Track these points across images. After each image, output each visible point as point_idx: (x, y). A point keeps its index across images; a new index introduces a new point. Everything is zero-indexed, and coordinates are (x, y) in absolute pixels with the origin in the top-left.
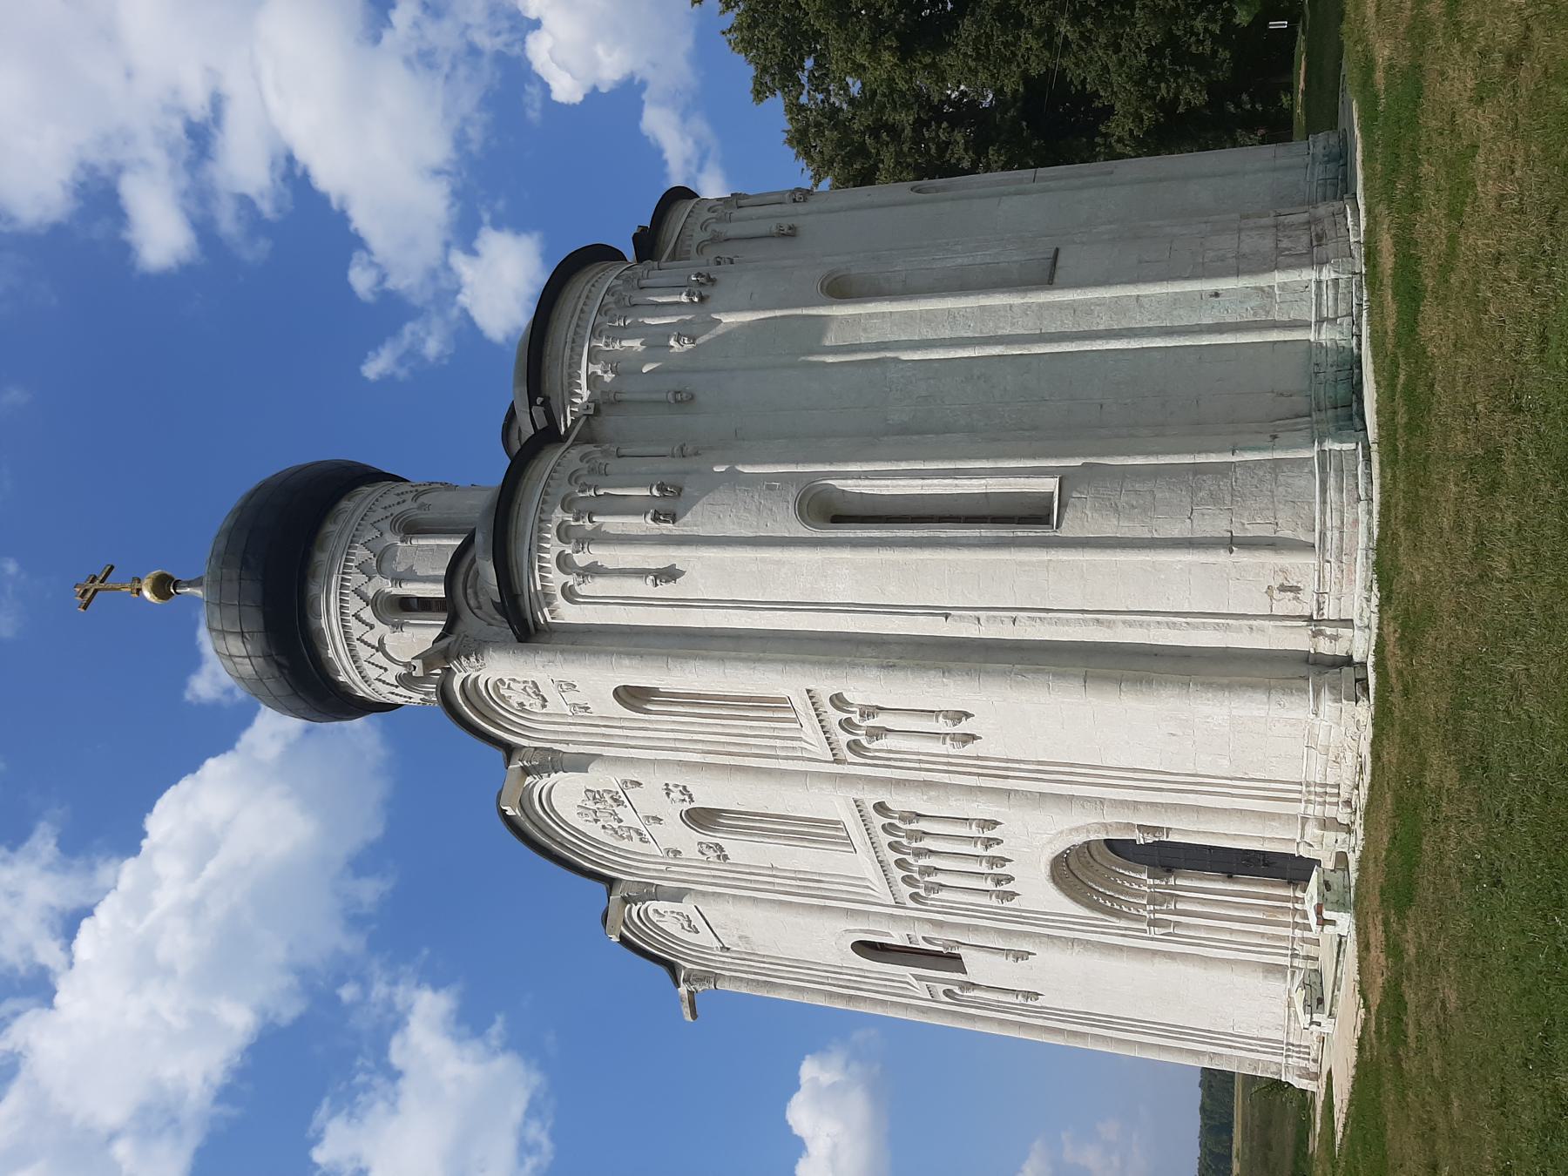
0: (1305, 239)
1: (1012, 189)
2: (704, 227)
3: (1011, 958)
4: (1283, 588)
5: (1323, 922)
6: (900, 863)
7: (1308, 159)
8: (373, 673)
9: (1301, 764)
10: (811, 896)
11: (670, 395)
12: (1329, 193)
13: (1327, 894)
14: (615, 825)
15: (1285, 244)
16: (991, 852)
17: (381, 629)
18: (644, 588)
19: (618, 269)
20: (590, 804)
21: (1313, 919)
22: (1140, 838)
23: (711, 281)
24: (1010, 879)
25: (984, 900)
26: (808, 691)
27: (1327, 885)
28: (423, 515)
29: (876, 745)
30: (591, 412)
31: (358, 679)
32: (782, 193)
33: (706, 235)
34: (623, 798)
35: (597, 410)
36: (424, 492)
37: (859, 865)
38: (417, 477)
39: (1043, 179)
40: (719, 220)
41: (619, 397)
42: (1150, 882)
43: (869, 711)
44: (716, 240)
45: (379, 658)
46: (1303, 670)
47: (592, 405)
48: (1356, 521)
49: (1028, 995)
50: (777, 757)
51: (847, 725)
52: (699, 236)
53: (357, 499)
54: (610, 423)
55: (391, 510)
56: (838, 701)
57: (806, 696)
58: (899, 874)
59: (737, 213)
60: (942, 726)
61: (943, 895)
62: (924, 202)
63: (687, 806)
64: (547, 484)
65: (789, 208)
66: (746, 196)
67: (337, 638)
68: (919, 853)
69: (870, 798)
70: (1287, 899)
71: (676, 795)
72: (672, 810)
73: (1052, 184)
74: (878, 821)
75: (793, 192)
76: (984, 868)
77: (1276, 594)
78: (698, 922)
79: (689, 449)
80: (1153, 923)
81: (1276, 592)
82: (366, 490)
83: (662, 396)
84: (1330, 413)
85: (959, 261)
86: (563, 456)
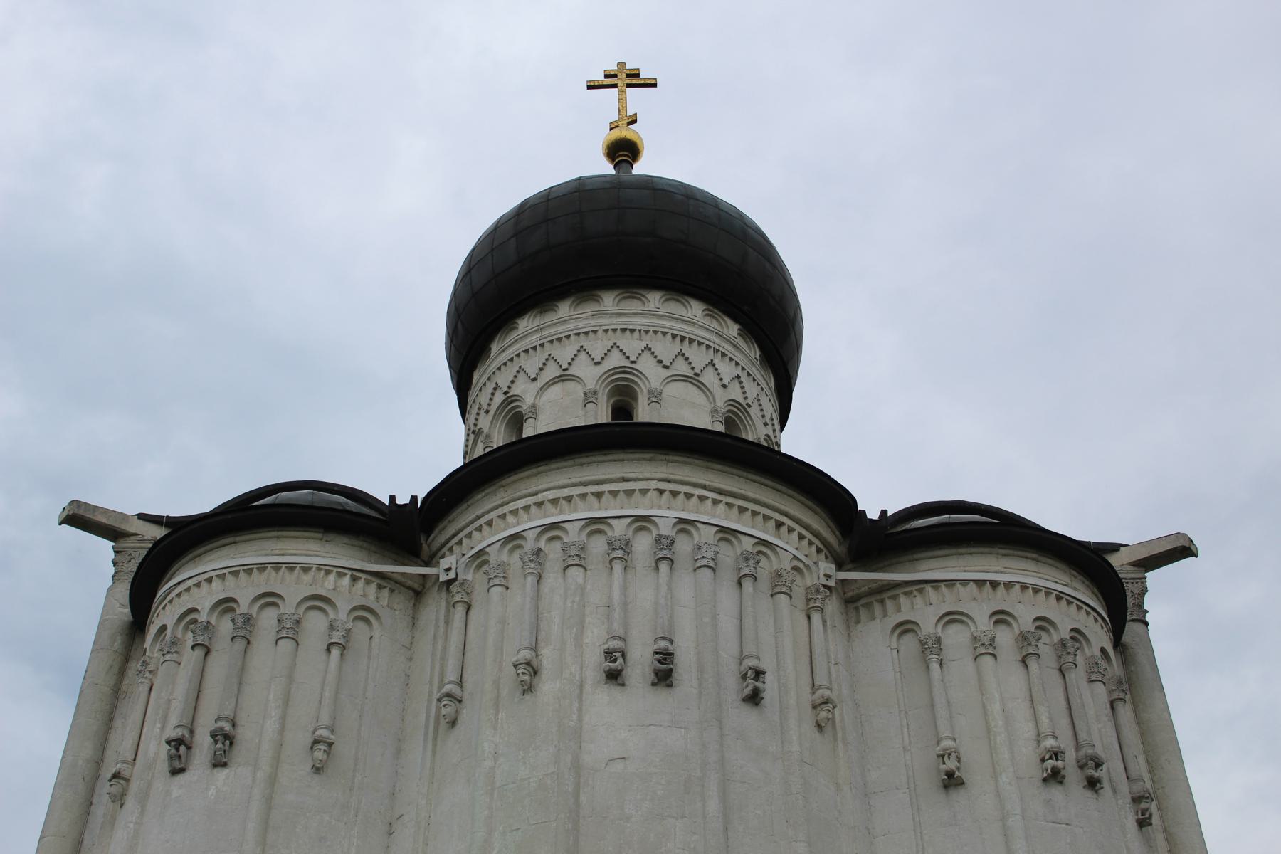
23: (664, 677)
45: (472, 436)
47: (452, 575)
64: (262, 567)
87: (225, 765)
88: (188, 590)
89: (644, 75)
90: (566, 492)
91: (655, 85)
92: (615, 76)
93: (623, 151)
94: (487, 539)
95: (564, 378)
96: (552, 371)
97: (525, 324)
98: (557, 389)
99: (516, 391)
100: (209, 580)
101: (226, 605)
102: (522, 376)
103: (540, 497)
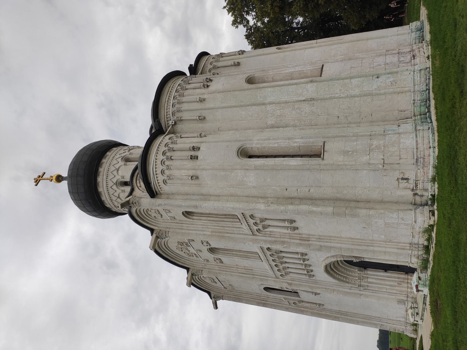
0: (409, 57)
1: (309, 46)
2: (211, 64)
3: (314, 295)
4: (403, 179)
5: (418, 291)
6: (276, 265)
7: (410, 31)
11: (198, 118)
12: (417, 41)
13: (420, 281)
14: (188, 252)
15: (402, 59)
17: (119, 191)
19: (183, 78)
20: (180, 246)
21: (415, 290)
22: (355, 261)
23: (211, 80)
24: (312, 271)
25: (304, 277)
26: (242, 213)
27: (420, 278)
28: (130, 156)
29: (266, 230)
30: (173, 124)
31: (113, 206)
32: (236, 52)
33: (211, 67)
35: (175, 123)
36: (132, 149)
37: (263, 266)
38: (131, 144)
39: (319, 43)
40: (216, 61)
41: (182, 118)
43: (262, 220)
44: (215, 67)
46: (411, 207)
47: (174, 122)
48: (429, 155)
49: (320, 305)
50: (234, 234)
51: (256, 224)
52: (210, 67)
53: (112, 152)
54: (179, 127)
55: (121, 155)
57: (242, 215)
58: (276, 269)
59: (221, 59)
60: (286, 224)
61: (291, 275)
62: (280, 52)
63: (209, 247)
64: (158, 147)
65: (238, 56)
66: (224, 54)
67: (106, 194)
68: (282, 263)
69: (265, 246)
70: (405, 279)
71: (205, 244)
72: (205, 248)
73: (322, 44)
74: (268, 253)
75: (239, 51)
77: (400, 181)
78: (216, 280)
79: (203, 135)
80: (360, 286)
81: (400, 180)
82: (115, 149)
83: (195, 118)
84: (419, 117)
85: (290, 71)
86: (164, 138)
87: (200, 148)
88: (156, 165)
89: (41, 175)
90: (168, 96)
91: (45, 173)
92: (37, 180)
93: (59, 179)
94: (171, 110)
95: (118, 170)
96: (115, 173)
97: (99, 179)
98: (119, 172)
99: (115, 180)
100: (156, 159)
101: (164, 153)
102: (112, 180)
103: (166, 101)
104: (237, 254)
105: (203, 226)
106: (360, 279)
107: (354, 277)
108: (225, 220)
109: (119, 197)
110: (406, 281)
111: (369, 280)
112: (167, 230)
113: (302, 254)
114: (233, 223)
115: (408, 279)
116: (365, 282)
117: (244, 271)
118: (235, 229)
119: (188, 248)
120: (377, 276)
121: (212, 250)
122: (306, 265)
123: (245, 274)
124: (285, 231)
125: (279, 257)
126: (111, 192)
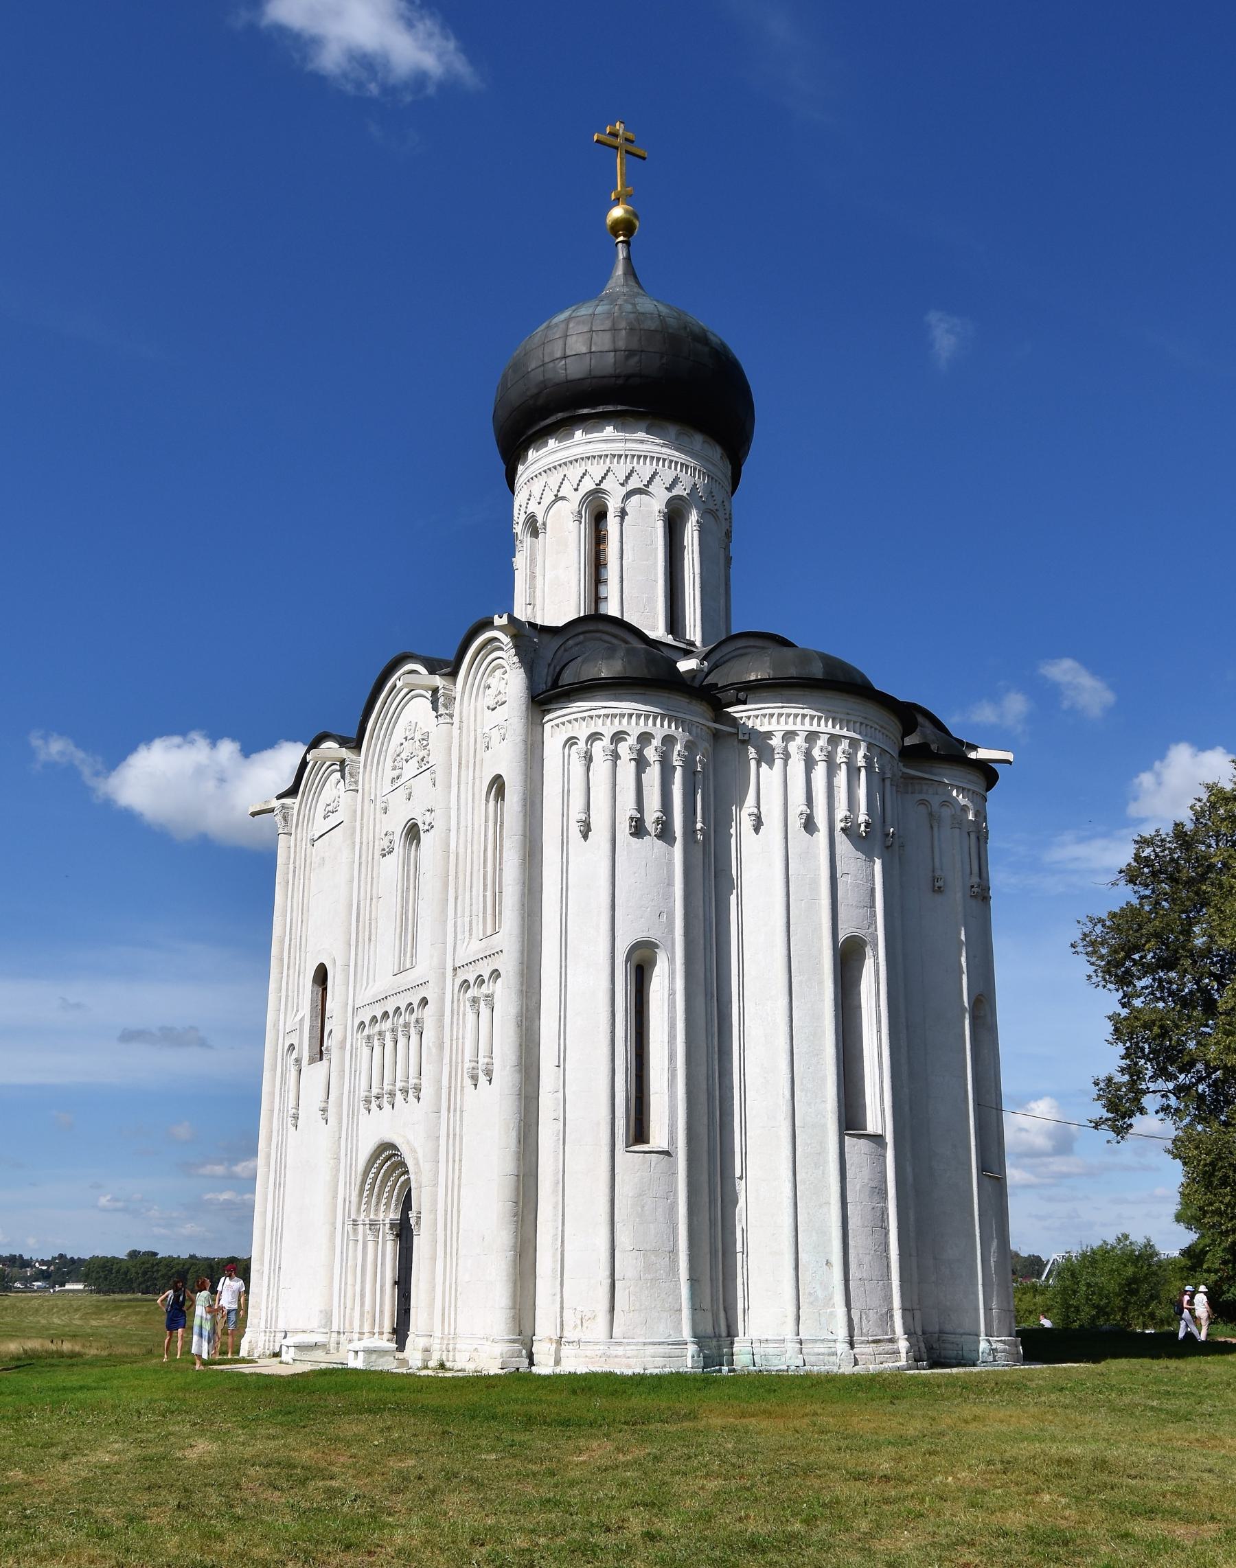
3: (323, 1105)
6: (386, 1014)
8: (536, 487)
9: (464, 1333)
10: (359, 932)
14: (403, 756)
16: (398, 1093)
18: (576, 813)
20: (418, 736)
34: (424, 768)
42: (387, 1221)
43: (489, 998)
49: (296, 1117)
51: (480, 981)
56: (496, 974)
63: (421, 826)
68: (393, 1030)
70: (381, 1326)
76: (387, 1087)
104: (407, 902)
105: (470, 829)
106: (373, 1224)
107: (377, 1210)
108: (489, 894)
109: (557, 498)
110: (376, 1330)
111: (371, 1245)
112: (456, 725)
113: (418, 1089)
114: (481, 915)
115: (381, 1333)
116: (365, 1236)
117: (365, 915)
118: (467, 919)
119: (414, 763)
120: (383, 1264)
121: (413, 832)
122: (392, 1094)
123: (358, 921)
124: (468, 1057)
125: (406, 1025)
126: (574, 472)
